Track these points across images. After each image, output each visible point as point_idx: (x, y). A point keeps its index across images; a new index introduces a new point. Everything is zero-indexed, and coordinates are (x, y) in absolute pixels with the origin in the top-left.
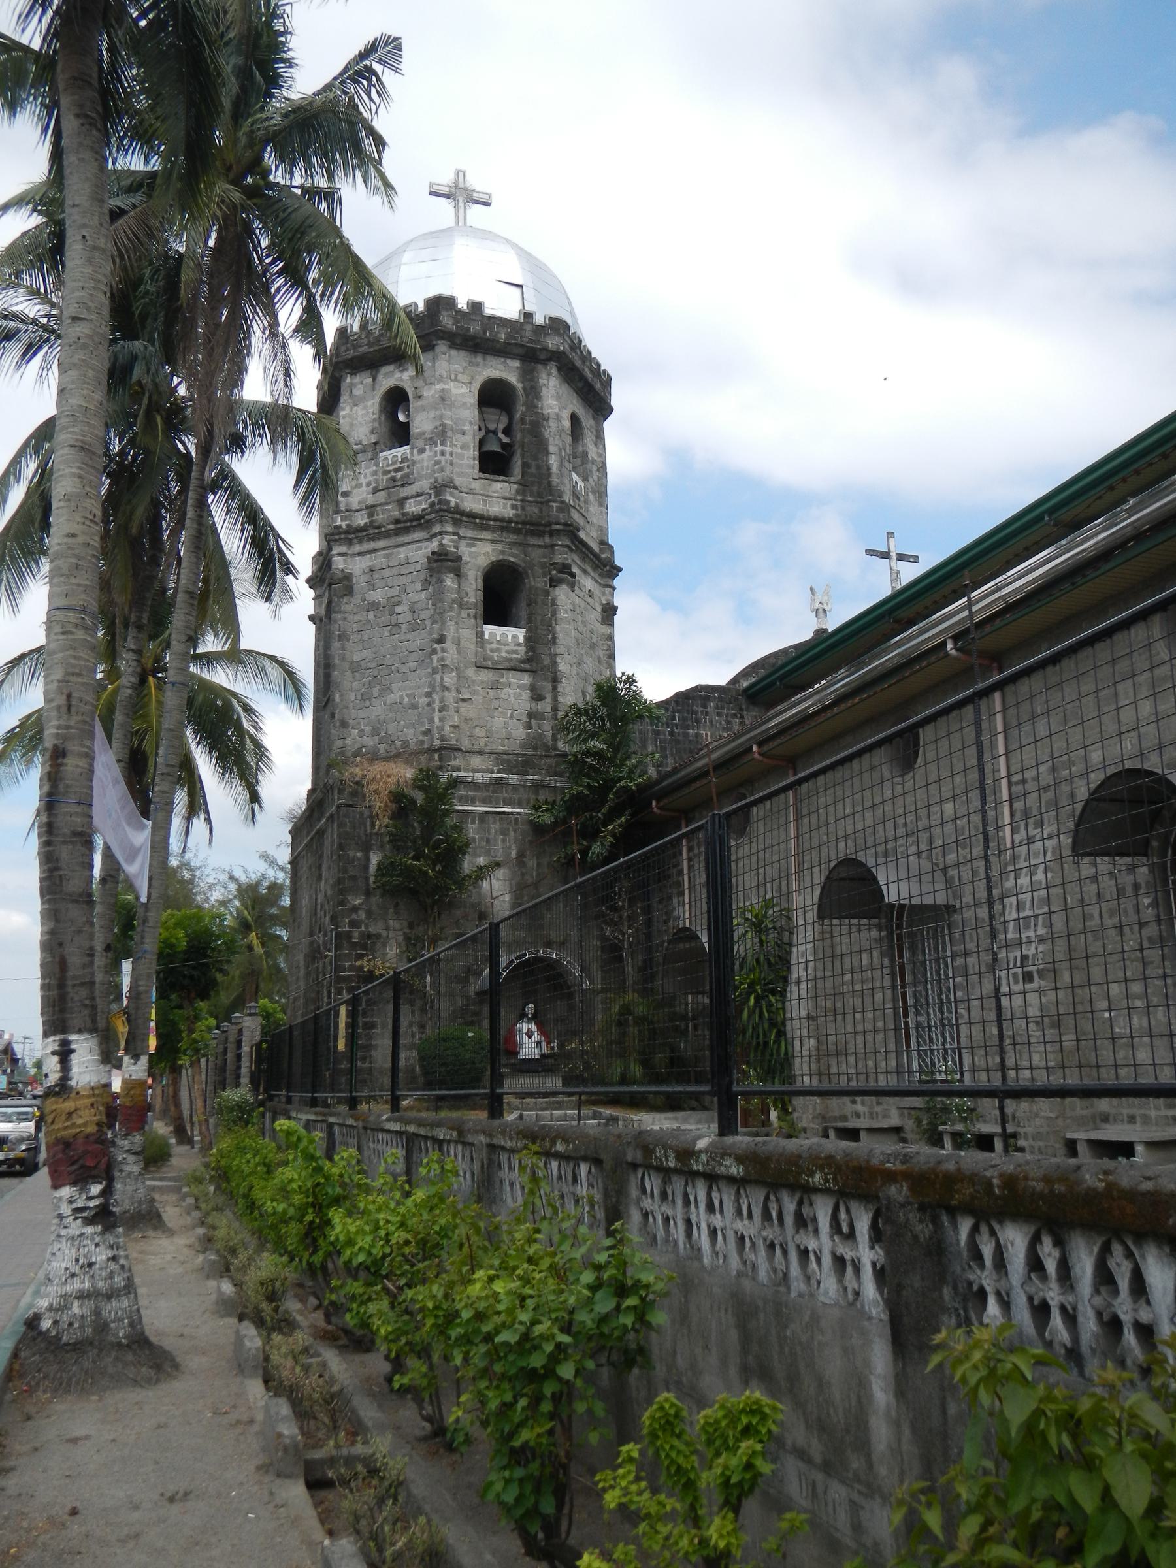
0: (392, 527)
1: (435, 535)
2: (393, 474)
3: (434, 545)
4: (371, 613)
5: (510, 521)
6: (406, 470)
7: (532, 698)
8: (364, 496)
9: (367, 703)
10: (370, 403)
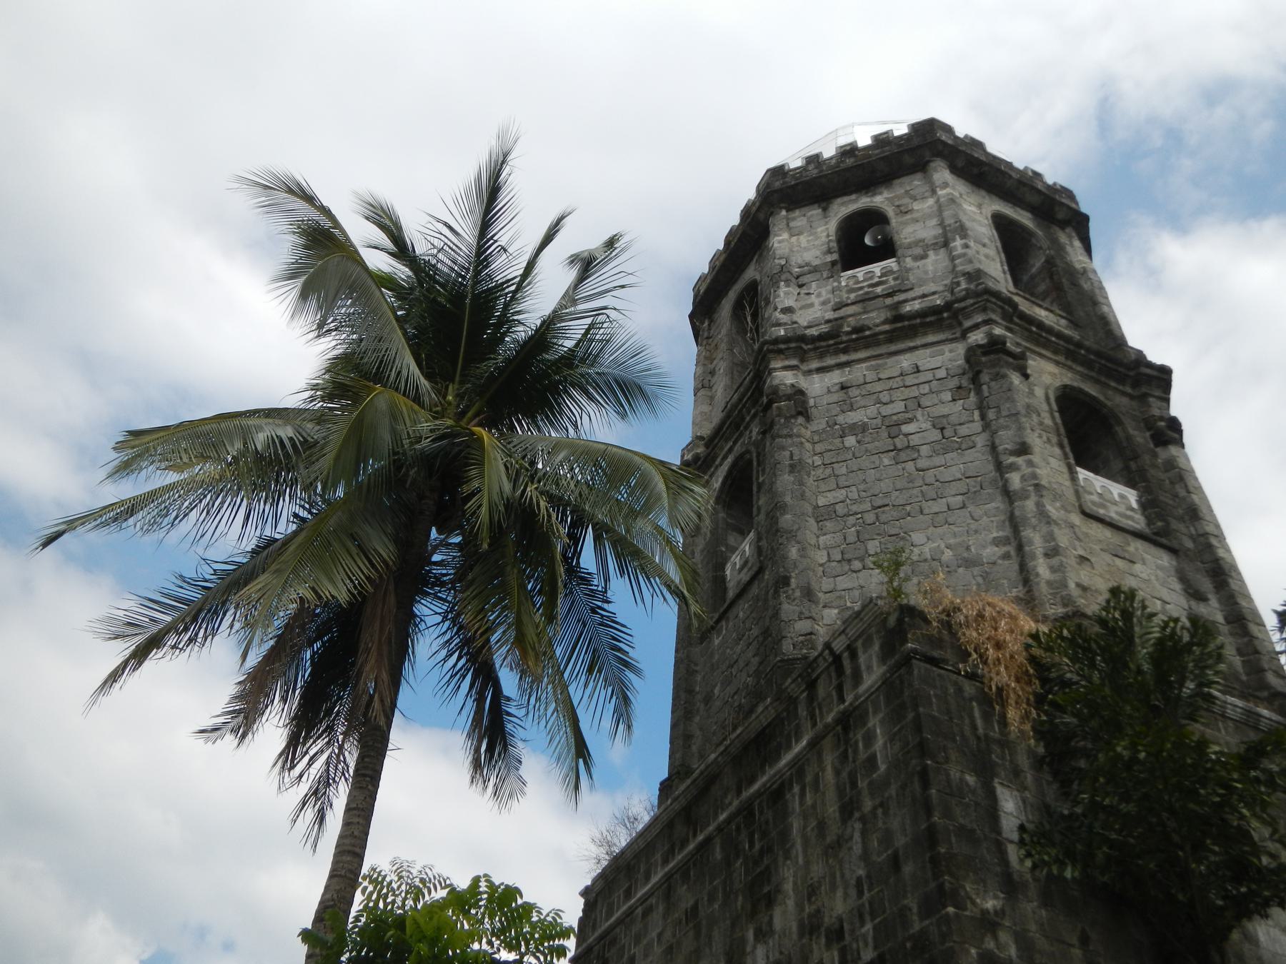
0: (887, 327)
1: (976, 327)
2: (866, 289)
3: (977, 337)
4: (851, 441)
5: (1079, 345)
6: (892, 283)
7: (1185, 591)
8: (819, 314)
9: (857, 565)
10: (819, 230)
